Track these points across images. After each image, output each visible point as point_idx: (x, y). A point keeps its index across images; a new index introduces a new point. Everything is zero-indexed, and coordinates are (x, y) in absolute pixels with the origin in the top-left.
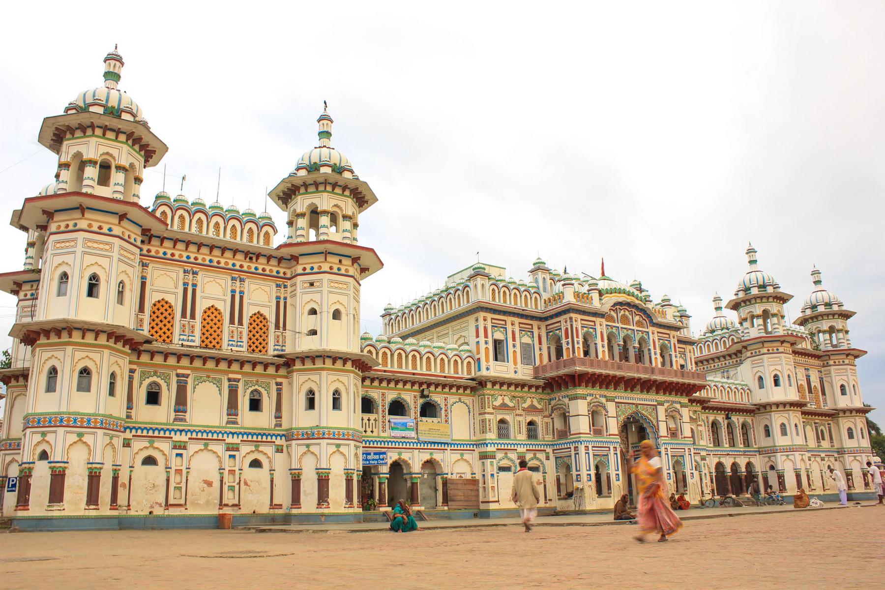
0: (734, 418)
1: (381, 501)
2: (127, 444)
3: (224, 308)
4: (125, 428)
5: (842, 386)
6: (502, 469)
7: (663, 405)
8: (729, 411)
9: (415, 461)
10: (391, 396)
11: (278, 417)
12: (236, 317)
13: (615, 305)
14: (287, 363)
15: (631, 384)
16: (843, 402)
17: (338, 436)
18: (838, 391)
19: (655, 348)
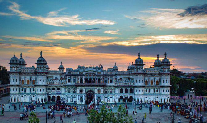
0: (128, 88)
1: (51, 101)
2: (20, 95)
3: (29, 79)
4: (19, 94)
5: (163, 81)
6: (69, 97)
7: (97, 88)
8: (125, 87)
9: (56, 96)
10: (52, 88)
11: (36, 91)
12: (31, 81)
13: (87, 74)
14: (36, 86)
15: (88, 86)
16: (163, 84)
17: (41, 94)
18: (163, 82)
19: (96, 79)
